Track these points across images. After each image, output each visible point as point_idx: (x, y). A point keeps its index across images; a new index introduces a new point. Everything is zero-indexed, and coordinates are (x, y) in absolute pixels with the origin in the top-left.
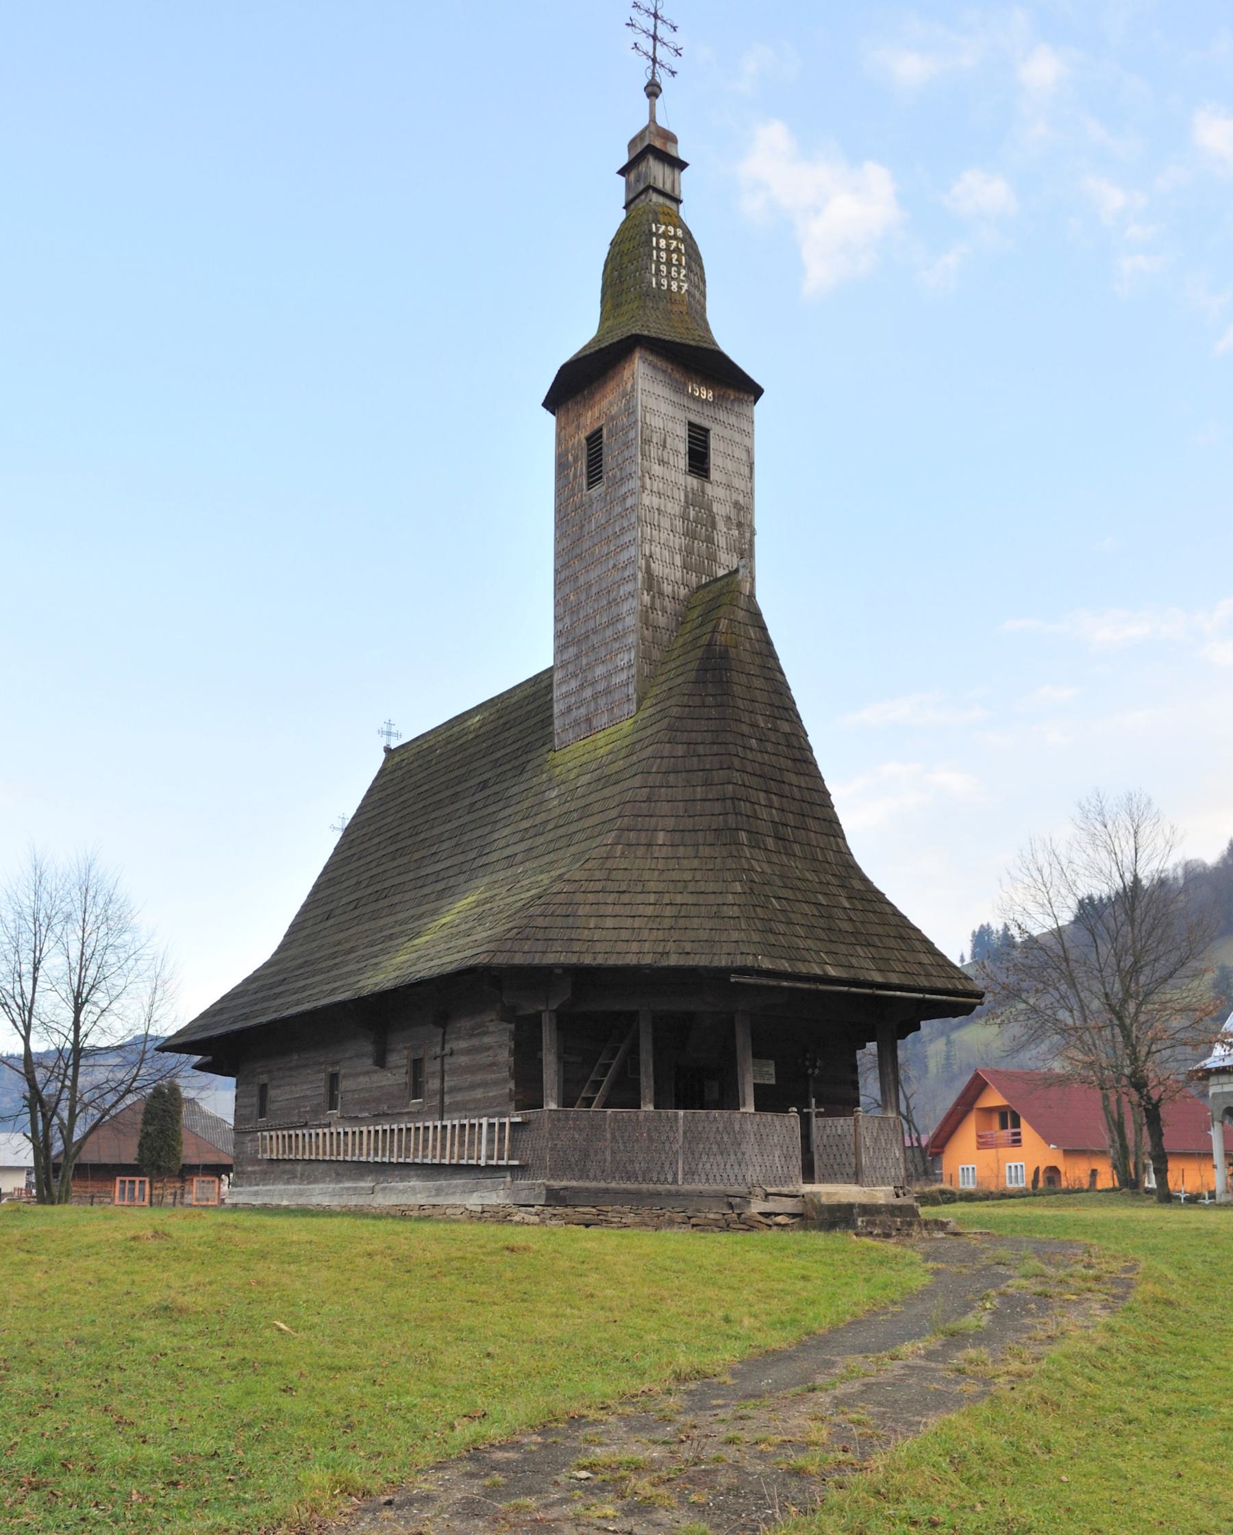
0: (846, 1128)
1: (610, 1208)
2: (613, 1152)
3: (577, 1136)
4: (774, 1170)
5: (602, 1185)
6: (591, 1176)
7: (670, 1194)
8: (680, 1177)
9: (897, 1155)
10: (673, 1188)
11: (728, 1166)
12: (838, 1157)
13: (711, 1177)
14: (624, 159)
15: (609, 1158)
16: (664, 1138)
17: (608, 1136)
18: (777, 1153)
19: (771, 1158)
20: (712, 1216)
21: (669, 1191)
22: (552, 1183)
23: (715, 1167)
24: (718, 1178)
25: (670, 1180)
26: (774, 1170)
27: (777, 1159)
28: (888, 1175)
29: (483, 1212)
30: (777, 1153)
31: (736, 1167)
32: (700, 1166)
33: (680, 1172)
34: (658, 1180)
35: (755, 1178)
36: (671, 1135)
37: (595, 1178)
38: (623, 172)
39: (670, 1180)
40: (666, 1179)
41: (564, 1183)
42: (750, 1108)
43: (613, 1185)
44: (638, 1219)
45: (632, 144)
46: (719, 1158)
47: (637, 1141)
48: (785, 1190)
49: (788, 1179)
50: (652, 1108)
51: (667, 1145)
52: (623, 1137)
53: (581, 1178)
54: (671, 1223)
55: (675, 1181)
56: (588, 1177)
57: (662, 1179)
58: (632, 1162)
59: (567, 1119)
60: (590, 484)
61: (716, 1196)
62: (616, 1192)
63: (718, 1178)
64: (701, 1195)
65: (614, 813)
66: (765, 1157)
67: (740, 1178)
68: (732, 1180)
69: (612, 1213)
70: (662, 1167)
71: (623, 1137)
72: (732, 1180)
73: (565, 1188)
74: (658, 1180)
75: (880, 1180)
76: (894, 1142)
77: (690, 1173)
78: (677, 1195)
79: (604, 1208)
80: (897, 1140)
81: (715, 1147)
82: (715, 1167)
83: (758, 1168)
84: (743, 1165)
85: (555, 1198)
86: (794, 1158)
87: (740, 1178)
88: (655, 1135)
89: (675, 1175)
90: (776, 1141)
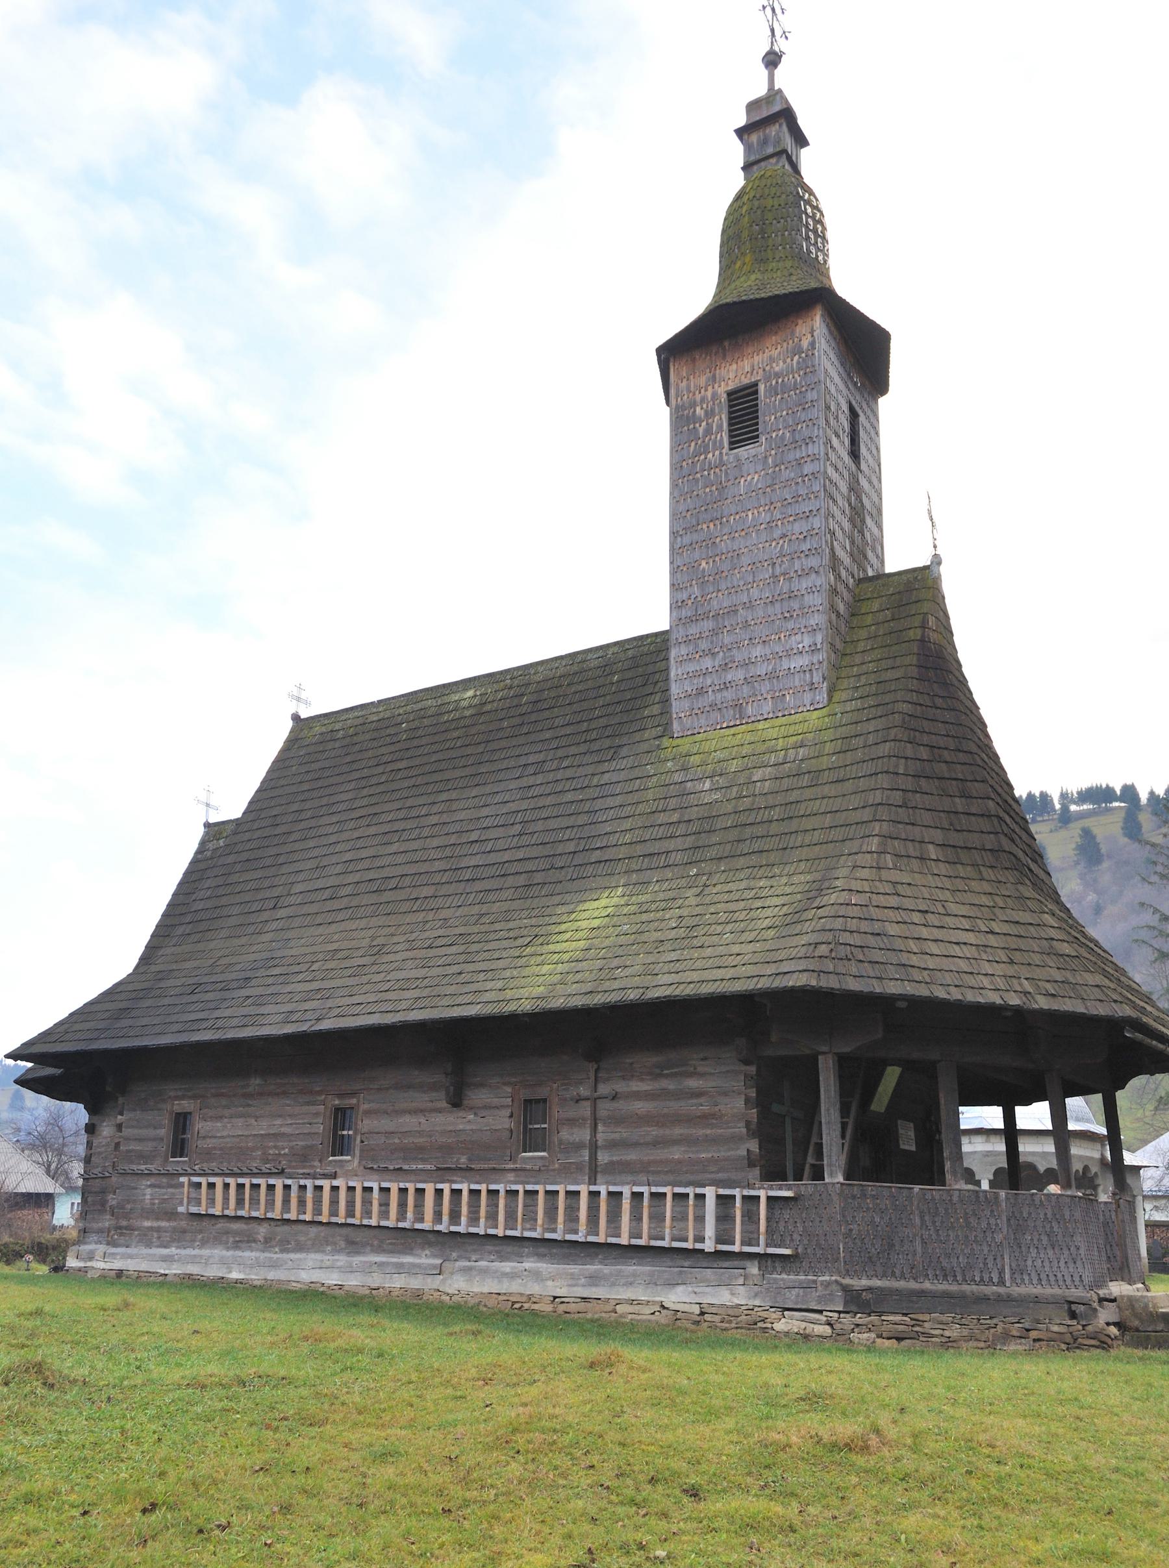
1: (926, 1317)
2: (924, 1242)
3: (877, 1219)
5: (913, 1285)
6: (898, 1273)
7: (999, 1299)
8: (1007, 1276)
10: (1001, 1290)
11: (1062, 1264)
13: (1043, 1276)
14: (742, 121)
15: (919, 1249)
16: (984, 1225)
17: (918, 1221)
20: (1056, 1328)
21: (999, 1295)
22: (847, 1281)
23: (1047, 1264)
24: (1052, 1279)
25: (995, 1280)
29: (702, 1314)
31: (1071, 1265)
32: (1029, 1263)
33: (1007, 1270)
34: (982, 1279)
36: (992, 1221)
37: (903, 1277)
38: (741, 133)
39: (995, 1280)
40: (991, 1279)
41: (865, 1282)
42: (835, 1177)
43: (927, 1285)
44: (965, 1332)
45: (752, 106)
46: (1050, 1252)
47: (953, 1228)
50: (840, 1179)
51: (989, 1234)
52: (934, 1222)
53: (884, 1276)
54: (1006, 1337)
55: (1002, 1283)
56: (893, 1274)
57: (986, 1277)
58: (948, 1256)
59: (864, 1196)
60: (736, 442)
61: (1054, 1302)
62: (933, 1295)
63: (1052, 1279)
64: (1037, 1300)
65: (866, 815)
67: (1077, 1279)
68: (1069, 1282)
69: (930, 1322)
70: (985, 1264)
71: (934, 1222)
72: (1069, 1282)
73: (869, 1289)
74: (982, 1279)
77: (1019, 1272)
78: (1009, 1299)
79: (920, 1317)
81: (1045, 1239)
82: (1047, 1264)
84: (1079, 1263)
85: (856, 1302)
87: (1077, 1279)
88: (973, 1221)
89: (1001, 1272)
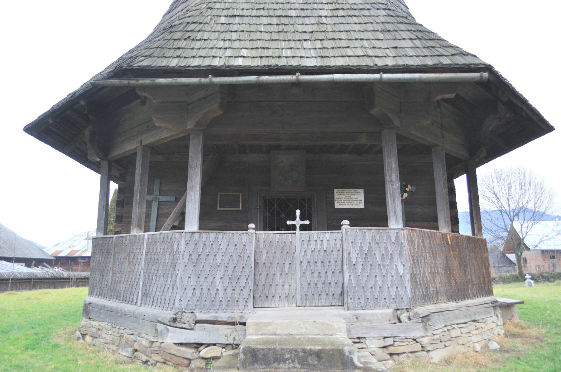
0: (332, 242)
4: (213, 292)
9: (401, 271)
12: (323, 274)
18: (219, 275)
19: (210, 279)
26: (213, 292)
27: (218, 280)
28: (385, 294)
30: (219, 275)
35: (184, 303)
48: (223, 316)
49: (230, 303)
66: (202, 279)
75: (371, 302)
76: (396, 256)
80: (400, 254)
83: (190, 292)
86: (243, 281)
90: (219, 261)
